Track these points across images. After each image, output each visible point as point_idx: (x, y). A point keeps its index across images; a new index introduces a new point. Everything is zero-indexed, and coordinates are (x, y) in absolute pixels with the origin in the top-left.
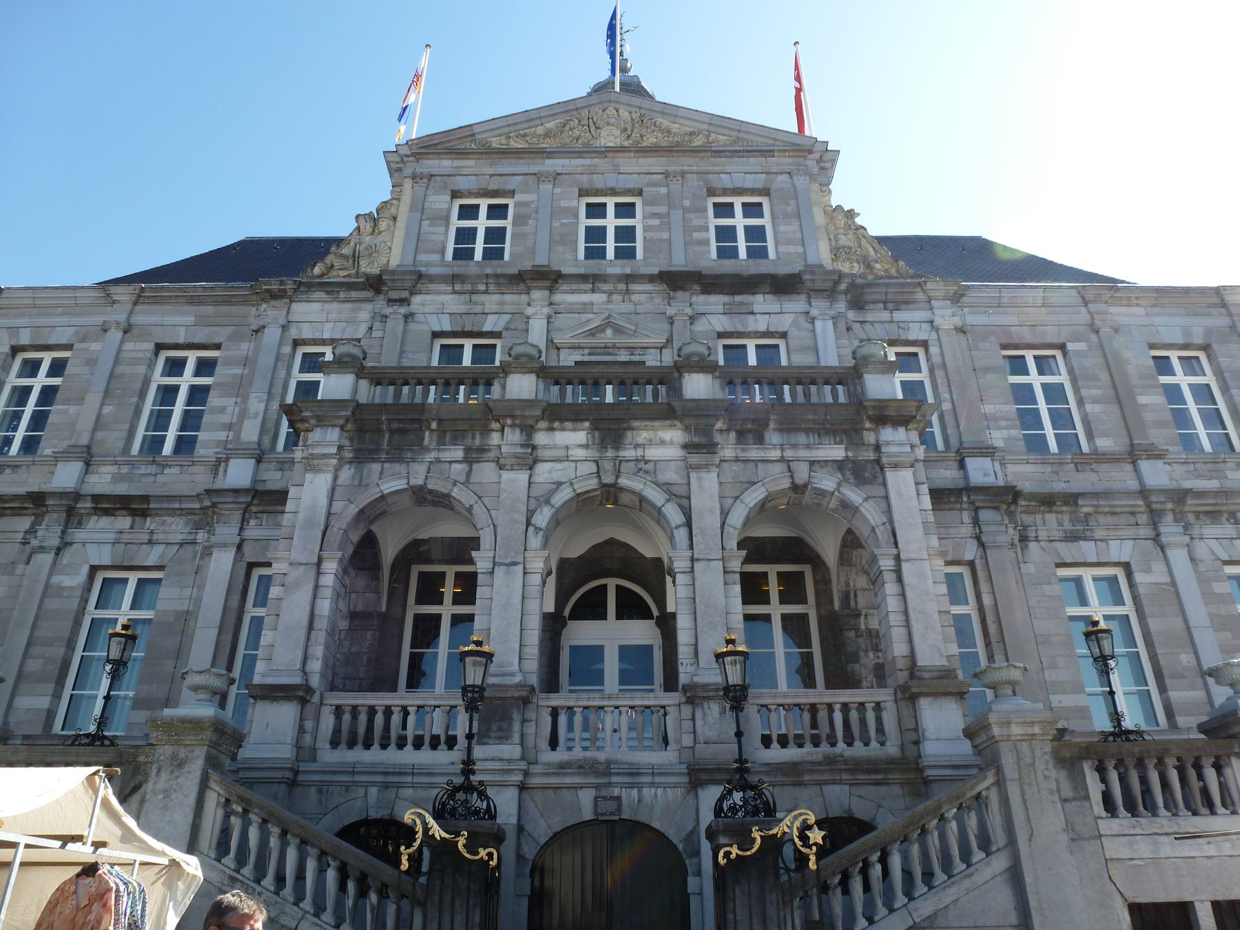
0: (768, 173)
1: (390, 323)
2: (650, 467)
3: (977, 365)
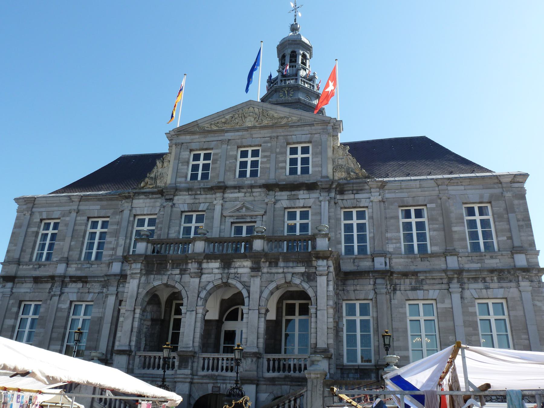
0: (311, 134)
1: (166, 209)
2: (239, 276)
3: (388, 216)
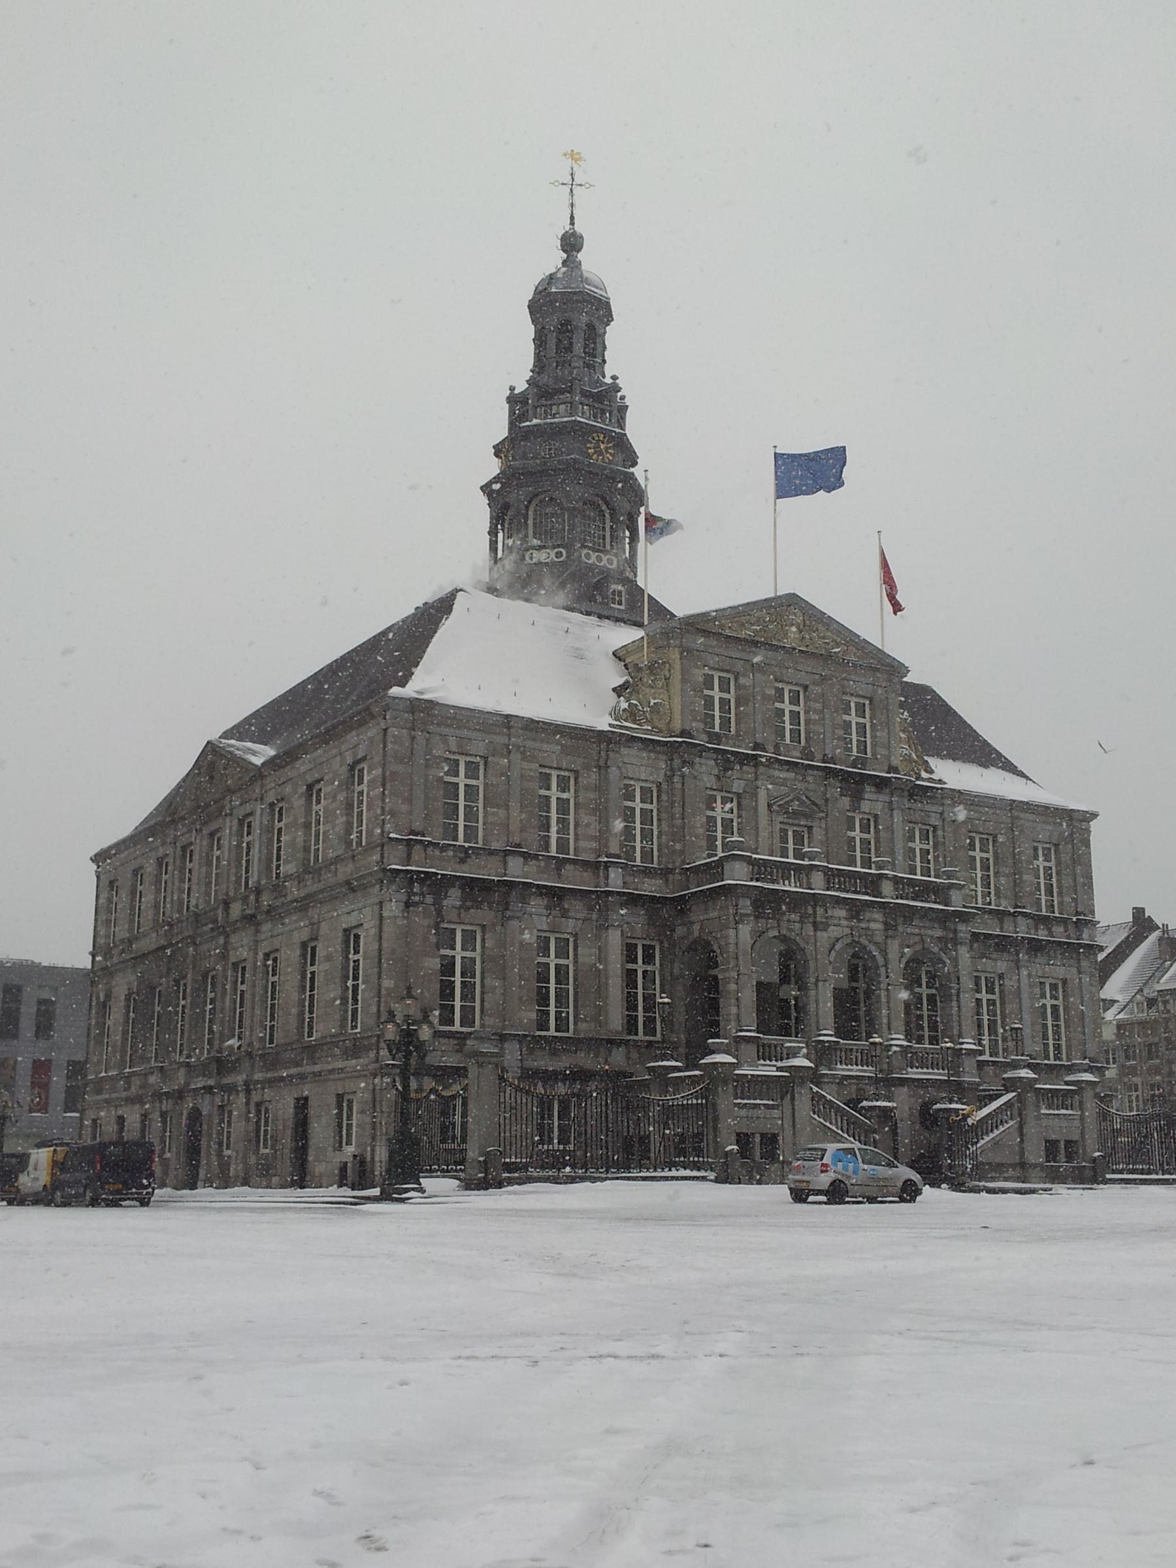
2: (870, 933)
